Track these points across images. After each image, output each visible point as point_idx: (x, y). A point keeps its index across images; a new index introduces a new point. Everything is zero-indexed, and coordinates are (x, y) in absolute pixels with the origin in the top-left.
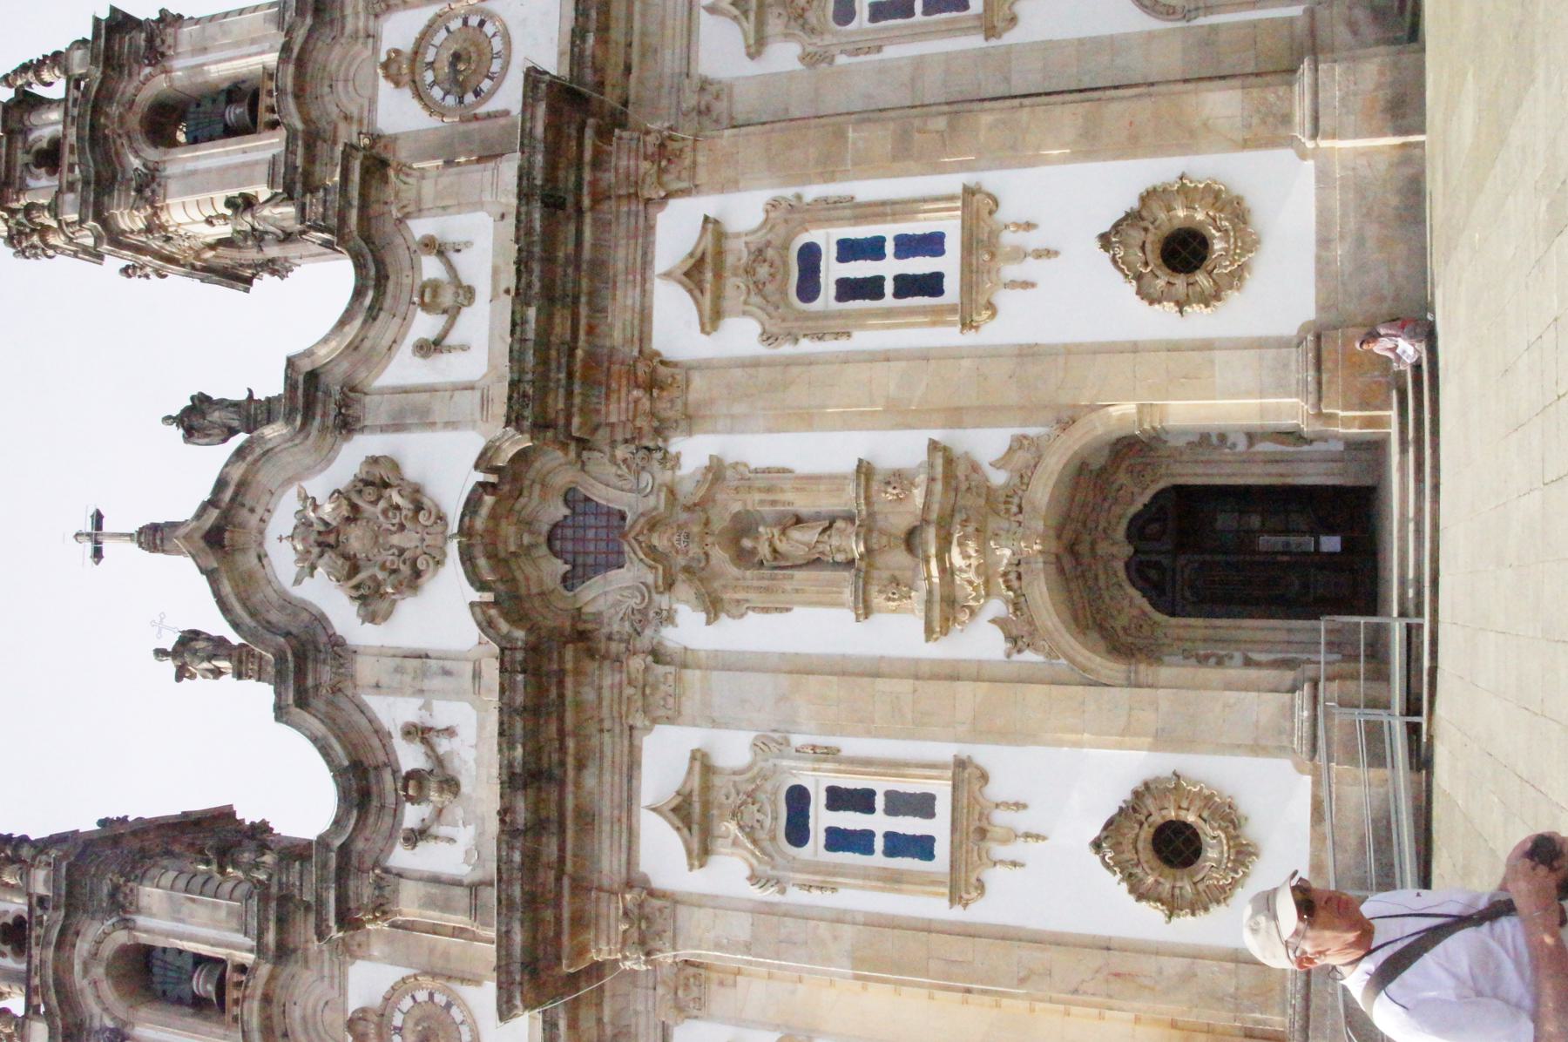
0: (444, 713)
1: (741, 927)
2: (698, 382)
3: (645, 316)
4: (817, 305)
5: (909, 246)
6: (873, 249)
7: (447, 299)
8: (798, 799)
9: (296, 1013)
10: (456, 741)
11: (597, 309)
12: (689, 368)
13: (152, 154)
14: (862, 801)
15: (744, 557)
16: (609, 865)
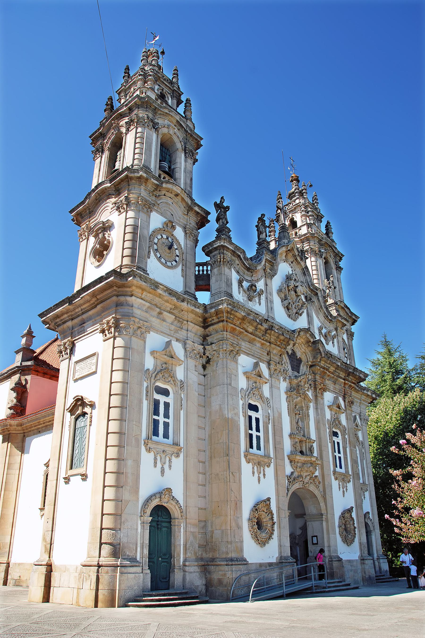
2: (322, 401)
9: (170, 201)
10: (258, 304)
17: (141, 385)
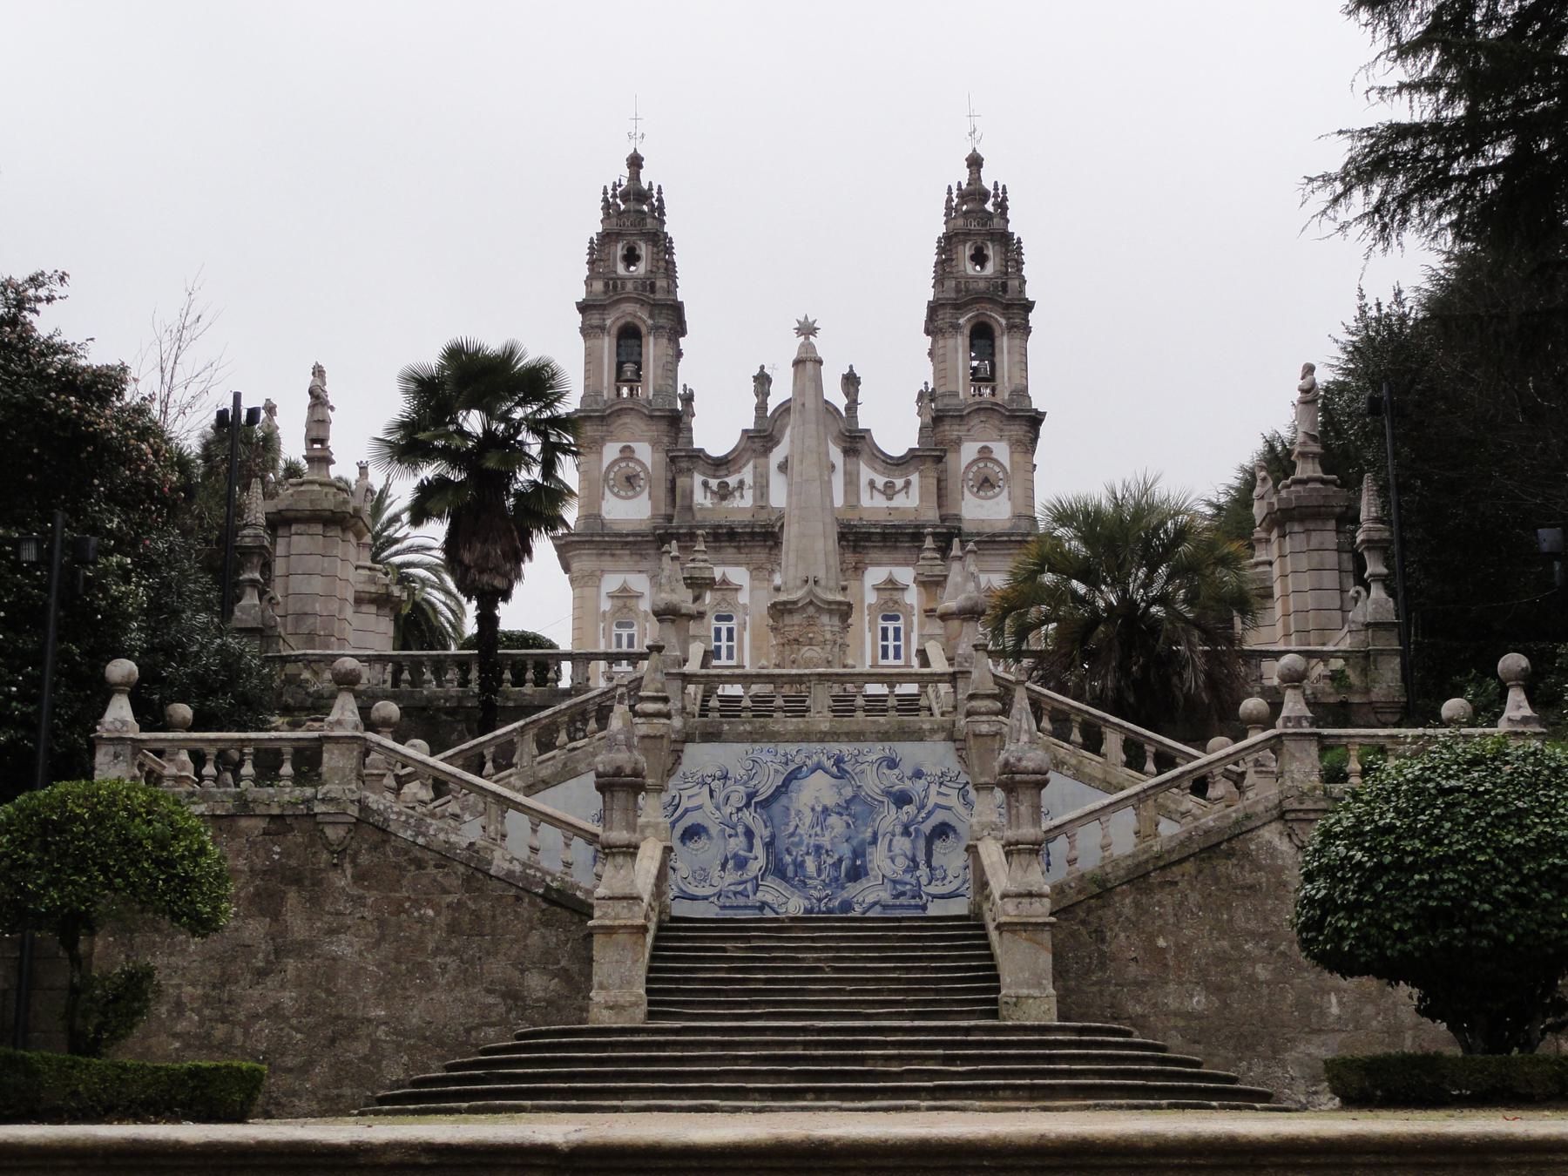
2: (857, 583)
3: (879, 564)
4: (880, 621)
5: (897, 649)
6: (897, 638)
7: (889, 492)
8: (729, 618)
11: (881, 548)
12: (862, 581)
14: (730, 638)
17: (597, 626)
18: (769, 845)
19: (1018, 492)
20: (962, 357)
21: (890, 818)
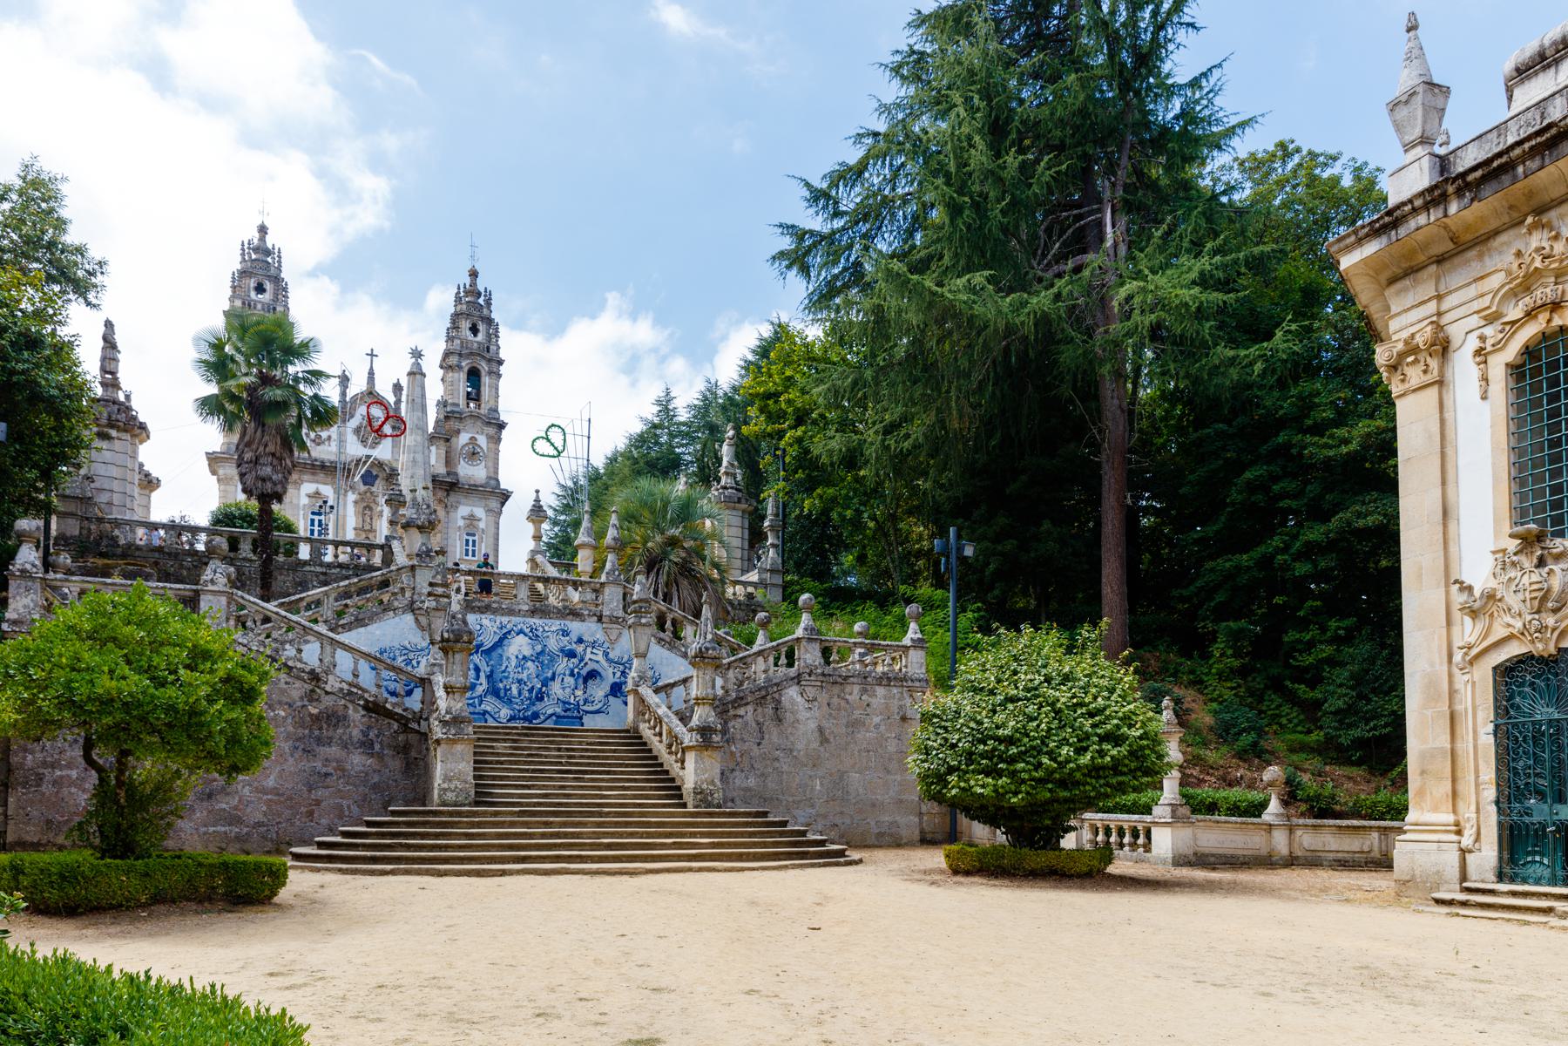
0: (333, 444)
1: (295, 501)
13: (466, 369)
15: (365, 508)
16: (305, 477)
18: (489, 677)
19: (490, 464)
20: (463, 387)
21: (563, 665)
